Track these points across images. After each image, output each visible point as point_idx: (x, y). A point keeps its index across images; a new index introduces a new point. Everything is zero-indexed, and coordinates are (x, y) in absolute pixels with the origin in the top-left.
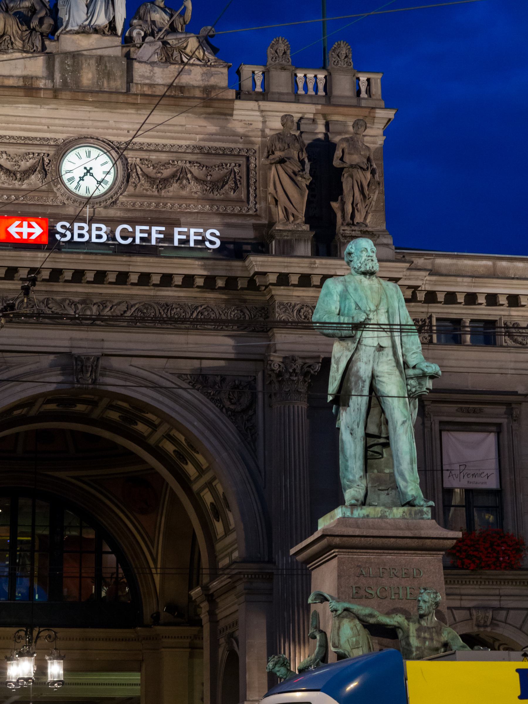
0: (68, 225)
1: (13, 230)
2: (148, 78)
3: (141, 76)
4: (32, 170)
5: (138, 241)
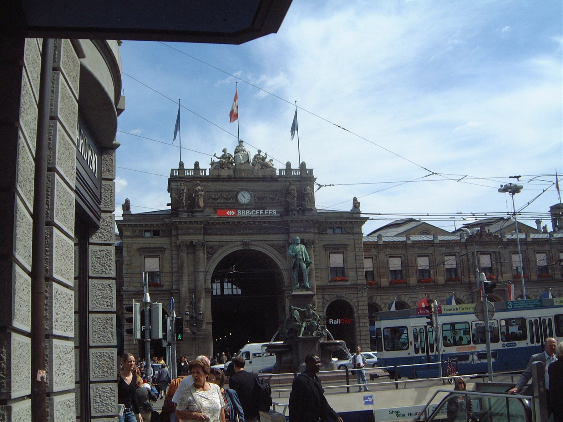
1: (228, 213)
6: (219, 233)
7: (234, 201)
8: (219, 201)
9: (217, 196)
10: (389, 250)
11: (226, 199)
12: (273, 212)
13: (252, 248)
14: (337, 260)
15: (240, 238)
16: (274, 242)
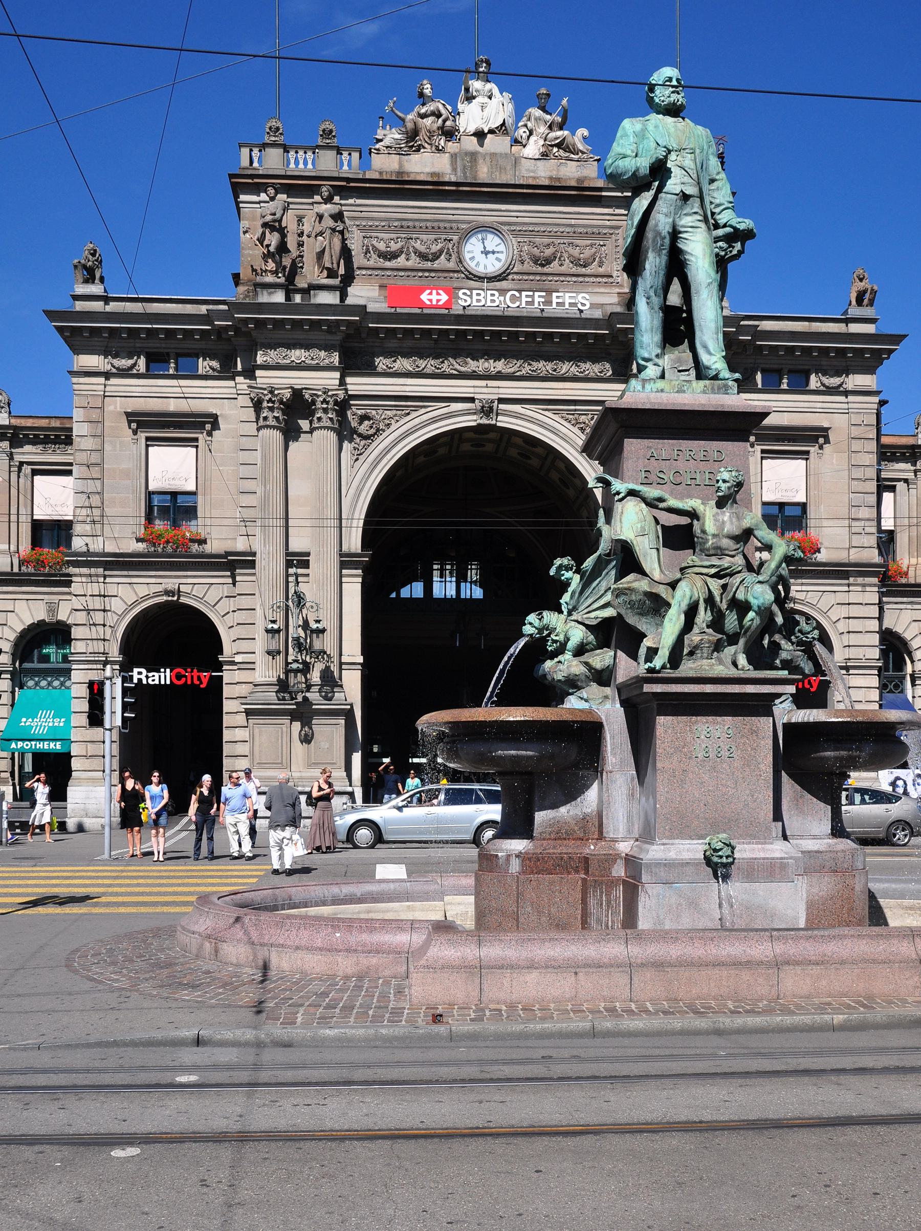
0: (469, 293)
2: (533, 172)
3: (526, 170)
4: (441, 252)
5: (524, 305)
7: (451, 265)
8: (401, 261)
9: (394, 247)
11: (423, 257)
13: (504, 422)
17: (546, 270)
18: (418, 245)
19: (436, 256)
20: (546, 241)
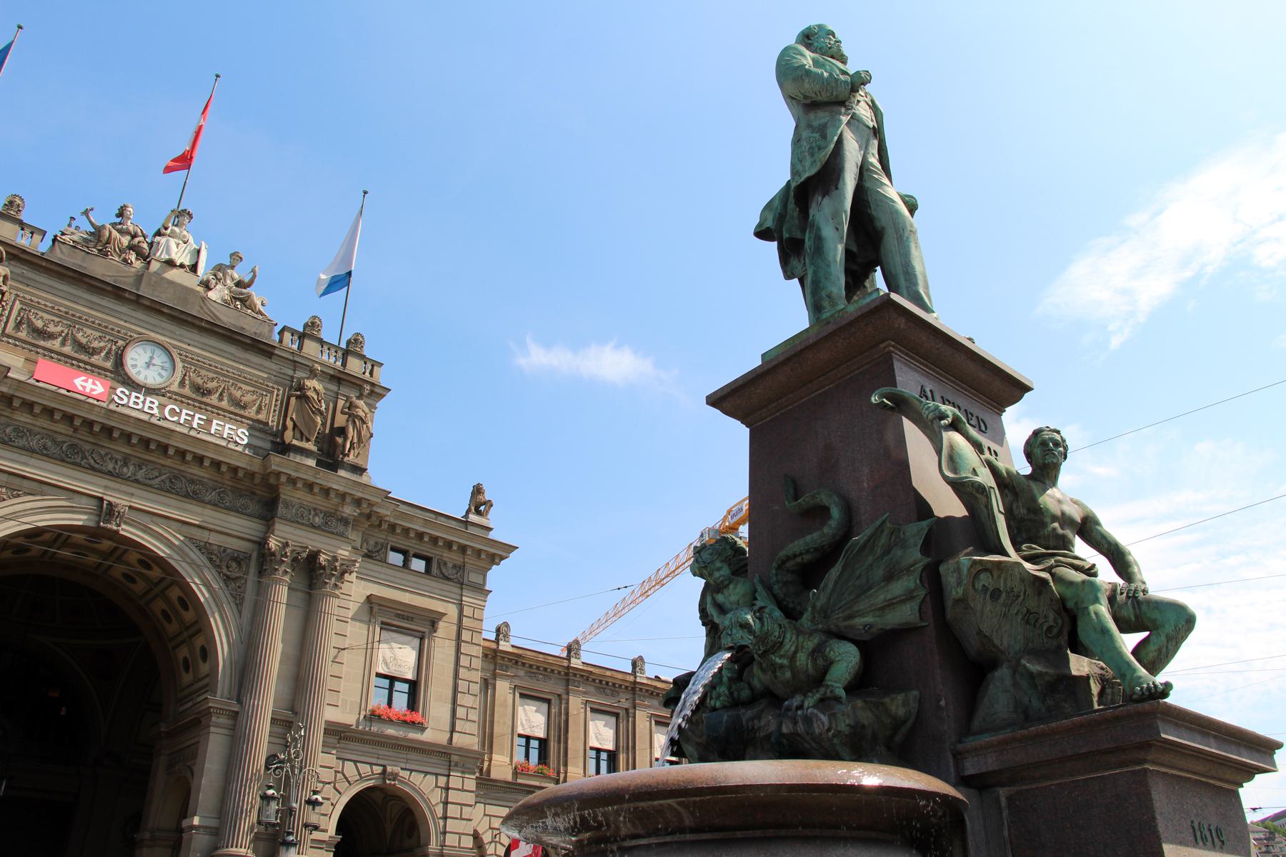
4: (102, 349)
6: (22, 442)
7: (109, 365)
8: (55, 344)
9: (52, 329)
10: (522, 673)
12: (232, 435)
13: (127, 531)
14: (400, 656)
15: (93, 486)
16: (214, 539)
17: (205, 399)
18: (79, 335)
19: (95, 352)
20: (211, 375)
